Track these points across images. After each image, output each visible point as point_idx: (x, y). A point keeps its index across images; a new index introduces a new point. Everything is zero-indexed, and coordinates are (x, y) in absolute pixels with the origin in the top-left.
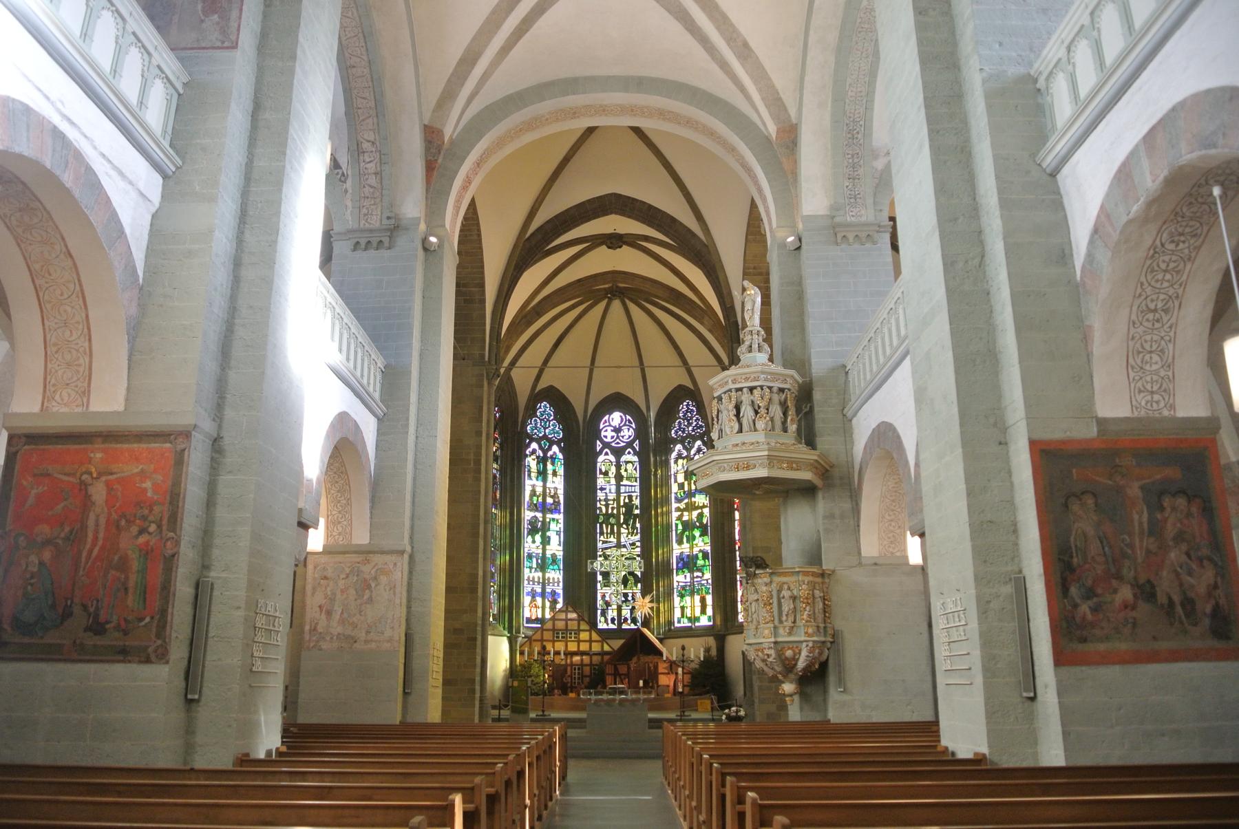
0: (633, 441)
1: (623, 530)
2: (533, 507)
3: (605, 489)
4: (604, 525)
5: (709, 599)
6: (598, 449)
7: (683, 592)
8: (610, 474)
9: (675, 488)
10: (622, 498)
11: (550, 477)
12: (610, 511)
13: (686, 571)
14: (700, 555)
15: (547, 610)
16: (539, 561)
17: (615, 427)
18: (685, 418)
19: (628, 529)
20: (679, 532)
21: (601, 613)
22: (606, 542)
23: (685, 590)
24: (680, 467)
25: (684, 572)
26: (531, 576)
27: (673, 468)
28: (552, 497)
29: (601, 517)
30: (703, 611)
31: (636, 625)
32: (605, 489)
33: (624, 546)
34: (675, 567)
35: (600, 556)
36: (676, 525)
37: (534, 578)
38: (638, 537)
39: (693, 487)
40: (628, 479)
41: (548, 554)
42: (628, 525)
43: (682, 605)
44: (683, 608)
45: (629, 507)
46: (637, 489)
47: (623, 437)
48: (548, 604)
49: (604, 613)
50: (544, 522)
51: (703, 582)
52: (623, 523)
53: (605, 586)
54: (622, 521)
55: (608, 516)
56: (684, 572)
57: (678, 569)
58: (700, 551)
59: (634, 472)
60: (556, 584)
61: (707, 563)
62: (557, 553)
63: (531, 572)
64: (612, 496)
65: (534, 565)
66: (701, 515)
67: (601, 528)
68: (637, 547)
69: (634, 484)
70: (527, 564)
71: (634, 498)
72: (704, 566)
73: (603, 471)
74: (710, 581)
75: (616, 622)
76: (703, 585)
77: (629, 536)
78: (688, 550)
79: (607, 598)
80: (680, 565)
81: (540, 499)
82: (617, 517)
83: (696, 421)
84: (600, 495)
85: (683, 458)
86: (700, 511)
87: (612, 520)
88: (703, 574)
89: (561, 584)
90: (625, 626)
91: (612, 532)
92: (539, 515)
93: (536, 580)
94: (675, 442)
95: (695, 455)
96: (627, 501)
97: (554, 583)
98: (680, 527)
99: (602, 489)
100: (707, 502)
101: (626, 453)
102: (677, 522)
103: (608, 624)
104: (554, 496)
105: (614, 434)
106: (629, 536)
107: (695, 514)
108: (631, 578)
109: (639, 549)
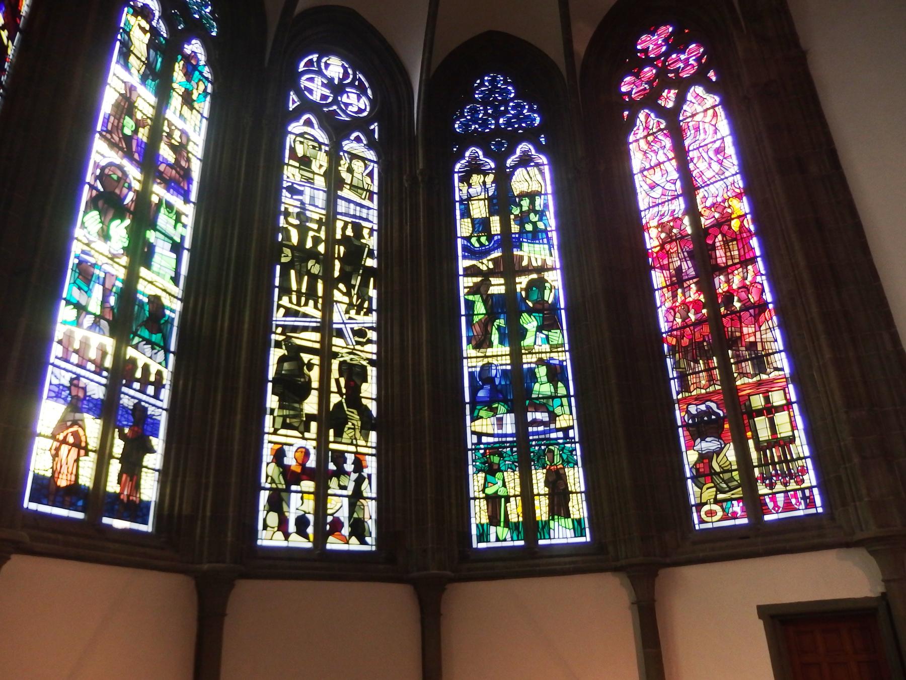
0: (369, 120)
1: (337, 295)
2: (125, 145)
3: (301, 193)
4: (293, 272)
5: (576, 478)
6: (291, 107)
7: (496, 459)
8: (315, 166)
9: (464, 228)
10: (339, 225)
11: (176, 100)
12: (309, 244)
13: (502, 409)
14: (542, 372)
15: (115, 467)
16: (112, 300)
17: (331, 80)
18: (485, 102)
19: (348, 294)
20: (476, 319)
21: (270, 500)
22: (296, 314)
23: (501, 455)
24: (476, 189)
25: (494, 411)
26: (79, 334)
27: (460, 190)
28: (173, 147)
29: (287, 251)
30: (559, 506)
31: (363, 542)
32: (301, 193)
33: (340, 334)
34: (467, 399)
35: (278, 345)
36: (470, 305)
37: (85, 344)
38: (373, 318)
39: (515, 228)
40: (353, 187)
41: (145, 290)
42: (350, 287)
43: (490, 491)
44: (494, 501)
45: (355, 250)
46: (374, 216)
47: (347, 105)
48: (118, 447)
49: (277, 503)
50: (143, 197)
51: (553, 435)
52: (340, 279)
53: (285, 426)
54: (337, 274)
55: (302, 255)
56: (494, 411)
57: (474, 402)
58: (540, 362)
59: (368, 180)
60: (151, 390)
61: (562, 391)
62: (166, 300)
63: (78, 323)
64: (316, 213)
65: (95, 306)
66: (539, 284)
67: (285, 276)
68: (369, 341)
69: (367, 203)
70: (70, 289)
71: (366, 232)
72: (552, 397)
73: (300, 153)
74: (574, 433)
75: (310, 530)
76: (555, 442)
77: (353, 313)
78: (507, 360)
79: (290, 460)
80: (481, 394)
81: (143, 134)
82: (326, 261)
83: (513, 108)
84: (288, 201)
85: (485, 173)
86: (535, 276)
87: (315, 268)
88: (553, 417)
89: (165, 394)
90: (333, 544)
91: (311, 293)
92: (134, 174)
93: (93, 354)
94: (468, 140)
95: (515, 168)
96: (349, 232)
97: (145, 382)
98: (480, 308)
99: (292, 190)
100: (554, 260)
101: (352, 137)
102: (471, 298)
103: (287, 536)
104: (179, 149)
105: (327, 92)
106: (353, 313)
107: (522, 281)
108: (355, 418)
109: (373, 348)
